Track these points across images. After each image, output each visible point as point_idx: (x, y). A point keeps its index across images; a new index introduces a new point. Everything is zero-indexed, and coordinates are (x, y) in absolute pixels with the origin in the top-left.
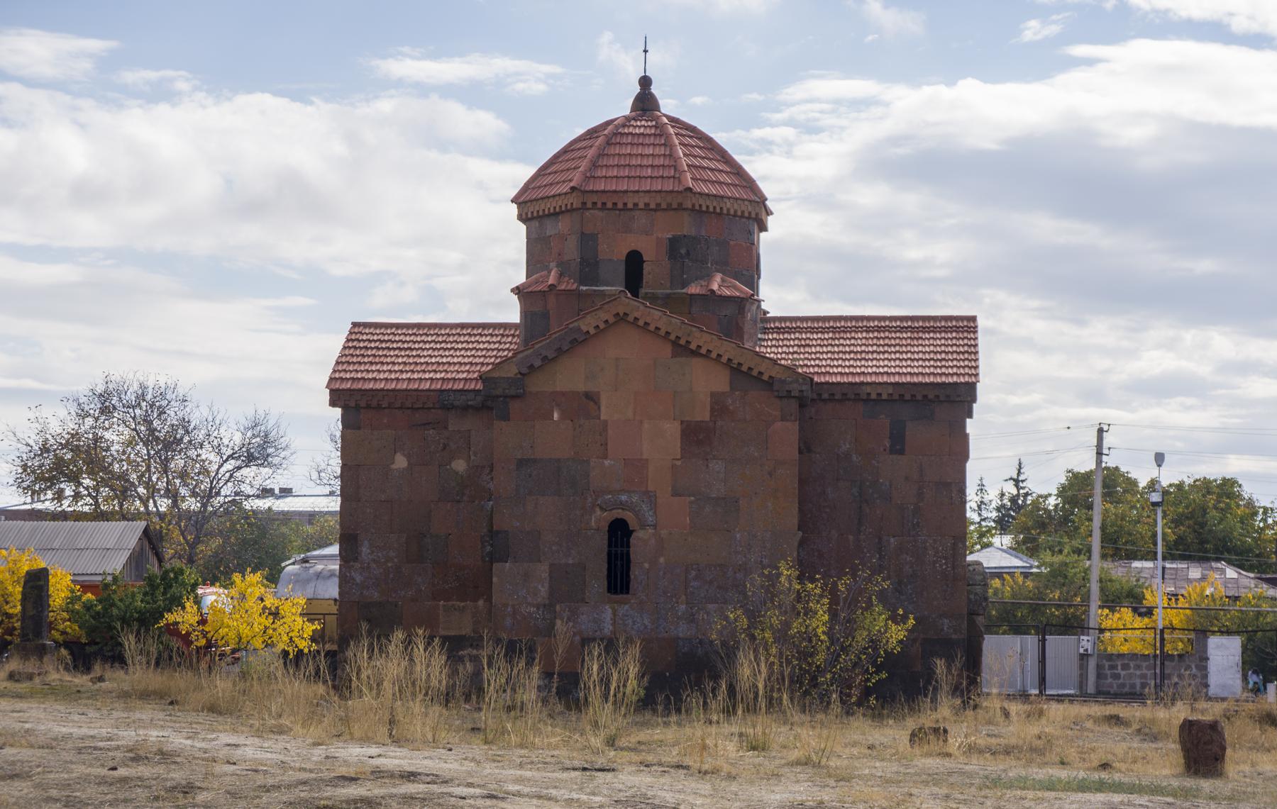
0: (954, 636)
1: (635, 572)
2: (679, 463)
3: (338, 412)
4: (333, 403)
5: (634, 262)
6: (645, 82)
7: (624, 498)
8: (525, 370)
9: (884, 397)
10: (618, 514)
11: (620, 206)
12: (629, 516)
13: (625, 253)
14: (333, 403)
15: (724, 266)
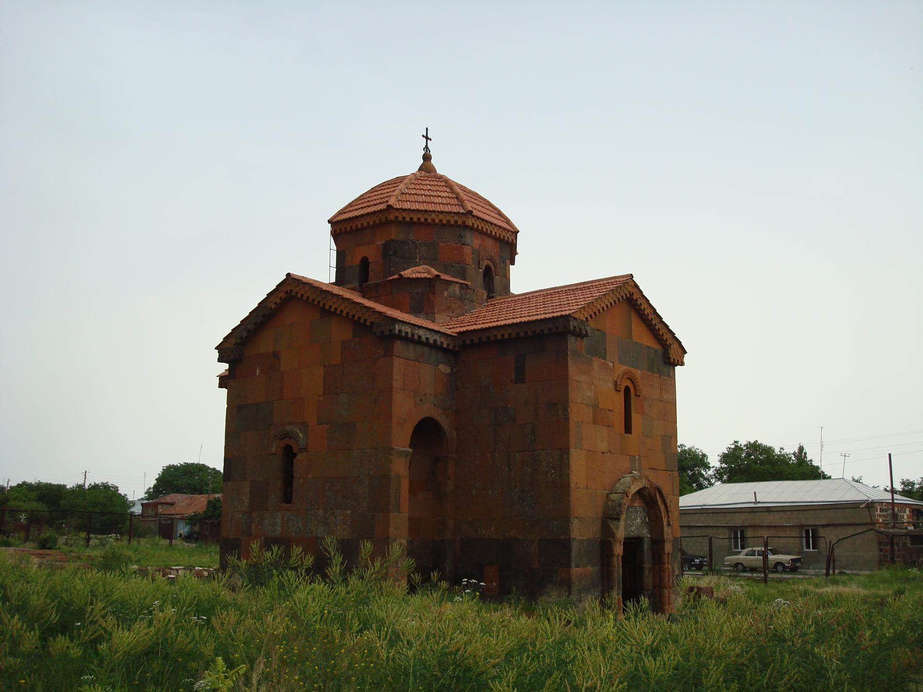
0: (562, 537)
1: (296, 485)
2: (321, 398)
3: (225, 391)
4: (221, 386)
5: (365, 262)
6: (427, 157)
7: (289, 428)
8: (238, 341)
9: (506, 336)
10: (287, 441)
11: (354, 228)
12: (291, 442)
13: (359, 258)
14: (221, 386)
15: (431, 261)
